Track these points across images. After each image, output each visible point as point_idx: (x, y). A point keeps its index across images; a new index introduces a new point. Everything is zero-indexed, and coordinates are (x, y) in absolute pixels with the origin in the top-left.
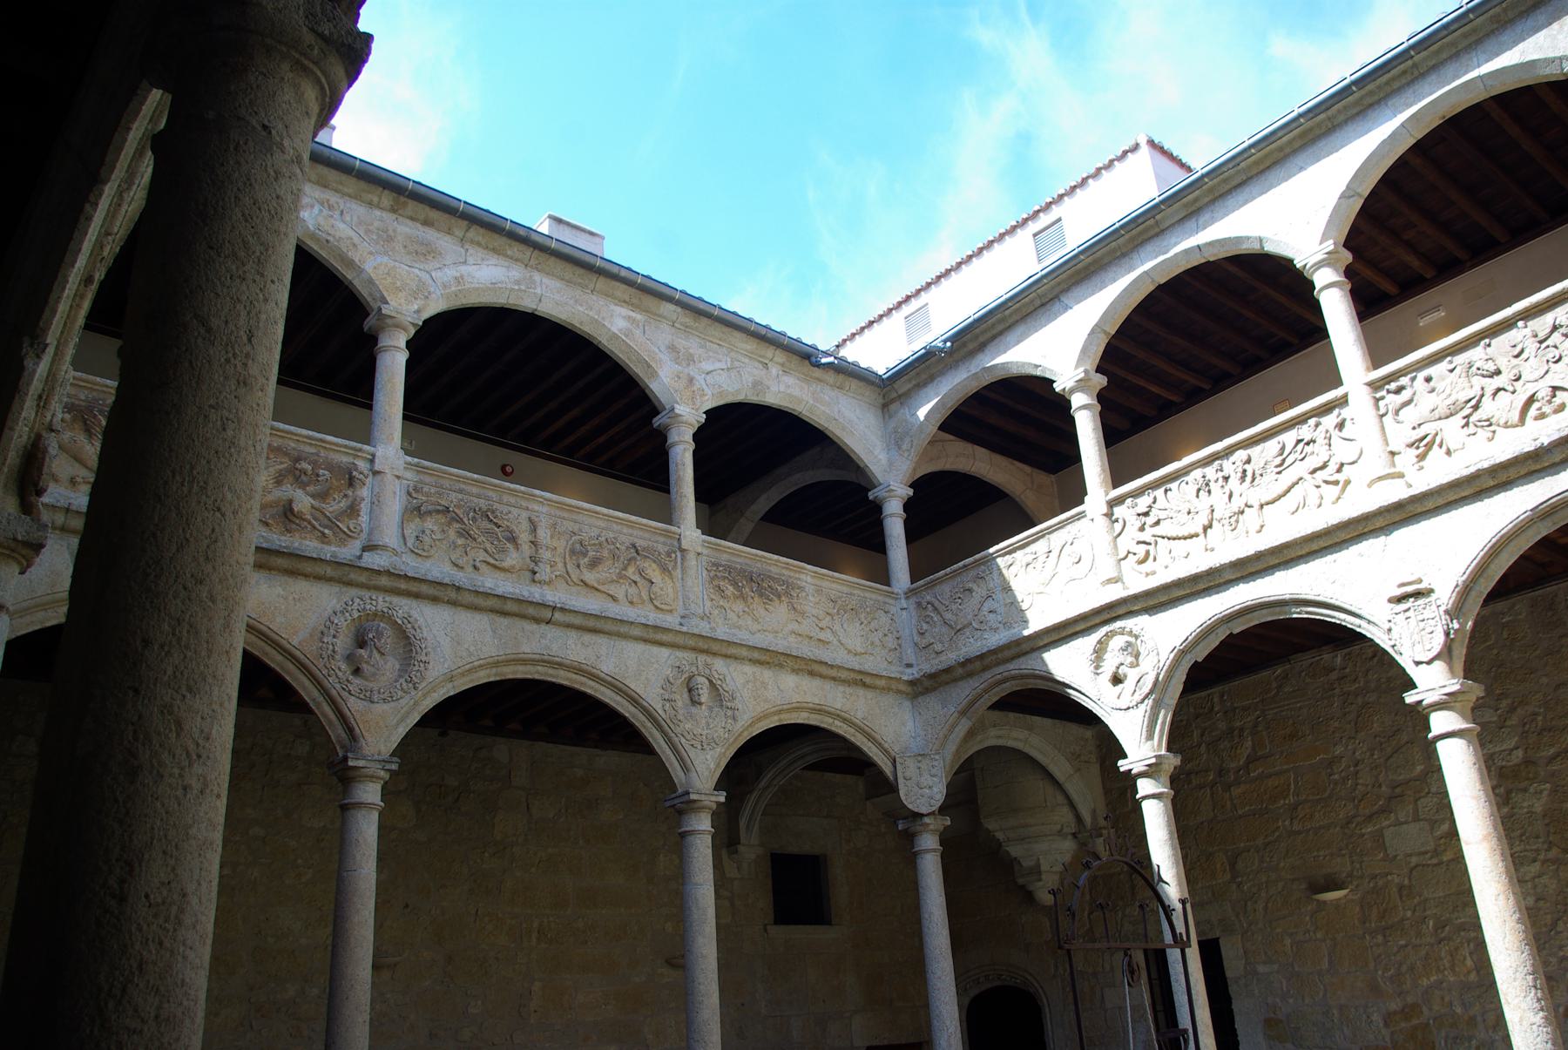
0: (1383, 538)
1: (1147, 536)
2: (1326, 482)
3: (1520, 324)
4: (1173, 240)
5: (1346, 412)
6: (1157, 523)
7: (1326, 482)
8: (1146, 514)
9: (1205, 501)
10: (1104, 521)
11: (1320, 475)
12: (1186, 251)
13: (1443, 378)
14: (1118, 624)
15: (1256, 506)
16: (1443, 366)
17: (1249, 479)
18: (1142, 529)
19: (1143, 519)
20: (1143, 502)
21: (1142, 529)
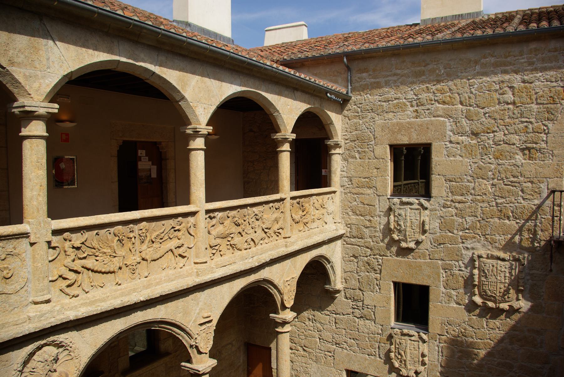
0: (201, 293)
1: (77, 265)
2: (180, 255)
3: (248, 208)
4: (142, 55)
5: (191, 219)
6: (85, 258)
7: (180, 255)
8: (78, 248)
9: (121, 252)
10: (45, 246)
11: (180, 251)
12: (146, 70)
13: (225, 220)
14: (51, 339)
15: (149, 260)
16: (226, 213)
17: (147, 242)
18: (74, 261)
19: (77, 251)
20: (77, 239)
21: (74, 261)
